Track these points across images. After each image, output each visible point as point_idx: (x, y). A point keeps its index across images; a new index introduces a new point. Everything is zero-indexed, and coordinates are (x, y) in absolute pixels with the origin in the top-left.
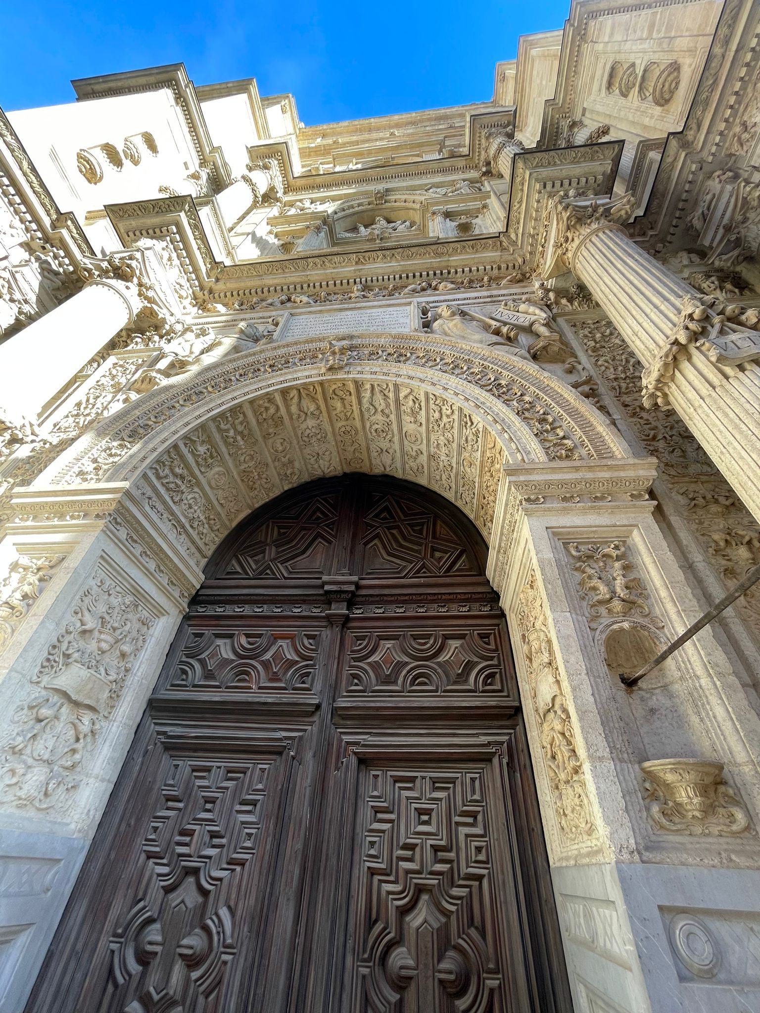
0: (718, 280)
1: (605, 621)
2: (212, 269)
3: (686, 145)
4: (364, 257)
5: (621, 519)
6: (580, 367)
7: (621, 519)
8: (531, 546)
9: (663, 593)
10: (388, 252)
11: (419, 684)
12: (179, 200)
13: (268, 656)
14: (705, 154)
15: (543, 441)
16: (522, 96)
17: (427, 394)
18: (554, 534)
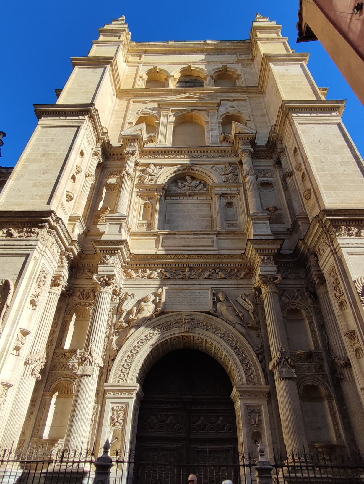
0: (310, 293)
2: (129, 255)
3: (305, 243)
4: (190, 256)
5: (259, 402)
7: (259, 402)
8: (240, 406)
9: (265, 423)
10: (199, 256)
11: (212, 431)
12: (122, 241)
13: (168, 422)
14: (310, 247)
15: (246, 374)
16: (264, 79)
17: (215, 345)
18: (246, 405)
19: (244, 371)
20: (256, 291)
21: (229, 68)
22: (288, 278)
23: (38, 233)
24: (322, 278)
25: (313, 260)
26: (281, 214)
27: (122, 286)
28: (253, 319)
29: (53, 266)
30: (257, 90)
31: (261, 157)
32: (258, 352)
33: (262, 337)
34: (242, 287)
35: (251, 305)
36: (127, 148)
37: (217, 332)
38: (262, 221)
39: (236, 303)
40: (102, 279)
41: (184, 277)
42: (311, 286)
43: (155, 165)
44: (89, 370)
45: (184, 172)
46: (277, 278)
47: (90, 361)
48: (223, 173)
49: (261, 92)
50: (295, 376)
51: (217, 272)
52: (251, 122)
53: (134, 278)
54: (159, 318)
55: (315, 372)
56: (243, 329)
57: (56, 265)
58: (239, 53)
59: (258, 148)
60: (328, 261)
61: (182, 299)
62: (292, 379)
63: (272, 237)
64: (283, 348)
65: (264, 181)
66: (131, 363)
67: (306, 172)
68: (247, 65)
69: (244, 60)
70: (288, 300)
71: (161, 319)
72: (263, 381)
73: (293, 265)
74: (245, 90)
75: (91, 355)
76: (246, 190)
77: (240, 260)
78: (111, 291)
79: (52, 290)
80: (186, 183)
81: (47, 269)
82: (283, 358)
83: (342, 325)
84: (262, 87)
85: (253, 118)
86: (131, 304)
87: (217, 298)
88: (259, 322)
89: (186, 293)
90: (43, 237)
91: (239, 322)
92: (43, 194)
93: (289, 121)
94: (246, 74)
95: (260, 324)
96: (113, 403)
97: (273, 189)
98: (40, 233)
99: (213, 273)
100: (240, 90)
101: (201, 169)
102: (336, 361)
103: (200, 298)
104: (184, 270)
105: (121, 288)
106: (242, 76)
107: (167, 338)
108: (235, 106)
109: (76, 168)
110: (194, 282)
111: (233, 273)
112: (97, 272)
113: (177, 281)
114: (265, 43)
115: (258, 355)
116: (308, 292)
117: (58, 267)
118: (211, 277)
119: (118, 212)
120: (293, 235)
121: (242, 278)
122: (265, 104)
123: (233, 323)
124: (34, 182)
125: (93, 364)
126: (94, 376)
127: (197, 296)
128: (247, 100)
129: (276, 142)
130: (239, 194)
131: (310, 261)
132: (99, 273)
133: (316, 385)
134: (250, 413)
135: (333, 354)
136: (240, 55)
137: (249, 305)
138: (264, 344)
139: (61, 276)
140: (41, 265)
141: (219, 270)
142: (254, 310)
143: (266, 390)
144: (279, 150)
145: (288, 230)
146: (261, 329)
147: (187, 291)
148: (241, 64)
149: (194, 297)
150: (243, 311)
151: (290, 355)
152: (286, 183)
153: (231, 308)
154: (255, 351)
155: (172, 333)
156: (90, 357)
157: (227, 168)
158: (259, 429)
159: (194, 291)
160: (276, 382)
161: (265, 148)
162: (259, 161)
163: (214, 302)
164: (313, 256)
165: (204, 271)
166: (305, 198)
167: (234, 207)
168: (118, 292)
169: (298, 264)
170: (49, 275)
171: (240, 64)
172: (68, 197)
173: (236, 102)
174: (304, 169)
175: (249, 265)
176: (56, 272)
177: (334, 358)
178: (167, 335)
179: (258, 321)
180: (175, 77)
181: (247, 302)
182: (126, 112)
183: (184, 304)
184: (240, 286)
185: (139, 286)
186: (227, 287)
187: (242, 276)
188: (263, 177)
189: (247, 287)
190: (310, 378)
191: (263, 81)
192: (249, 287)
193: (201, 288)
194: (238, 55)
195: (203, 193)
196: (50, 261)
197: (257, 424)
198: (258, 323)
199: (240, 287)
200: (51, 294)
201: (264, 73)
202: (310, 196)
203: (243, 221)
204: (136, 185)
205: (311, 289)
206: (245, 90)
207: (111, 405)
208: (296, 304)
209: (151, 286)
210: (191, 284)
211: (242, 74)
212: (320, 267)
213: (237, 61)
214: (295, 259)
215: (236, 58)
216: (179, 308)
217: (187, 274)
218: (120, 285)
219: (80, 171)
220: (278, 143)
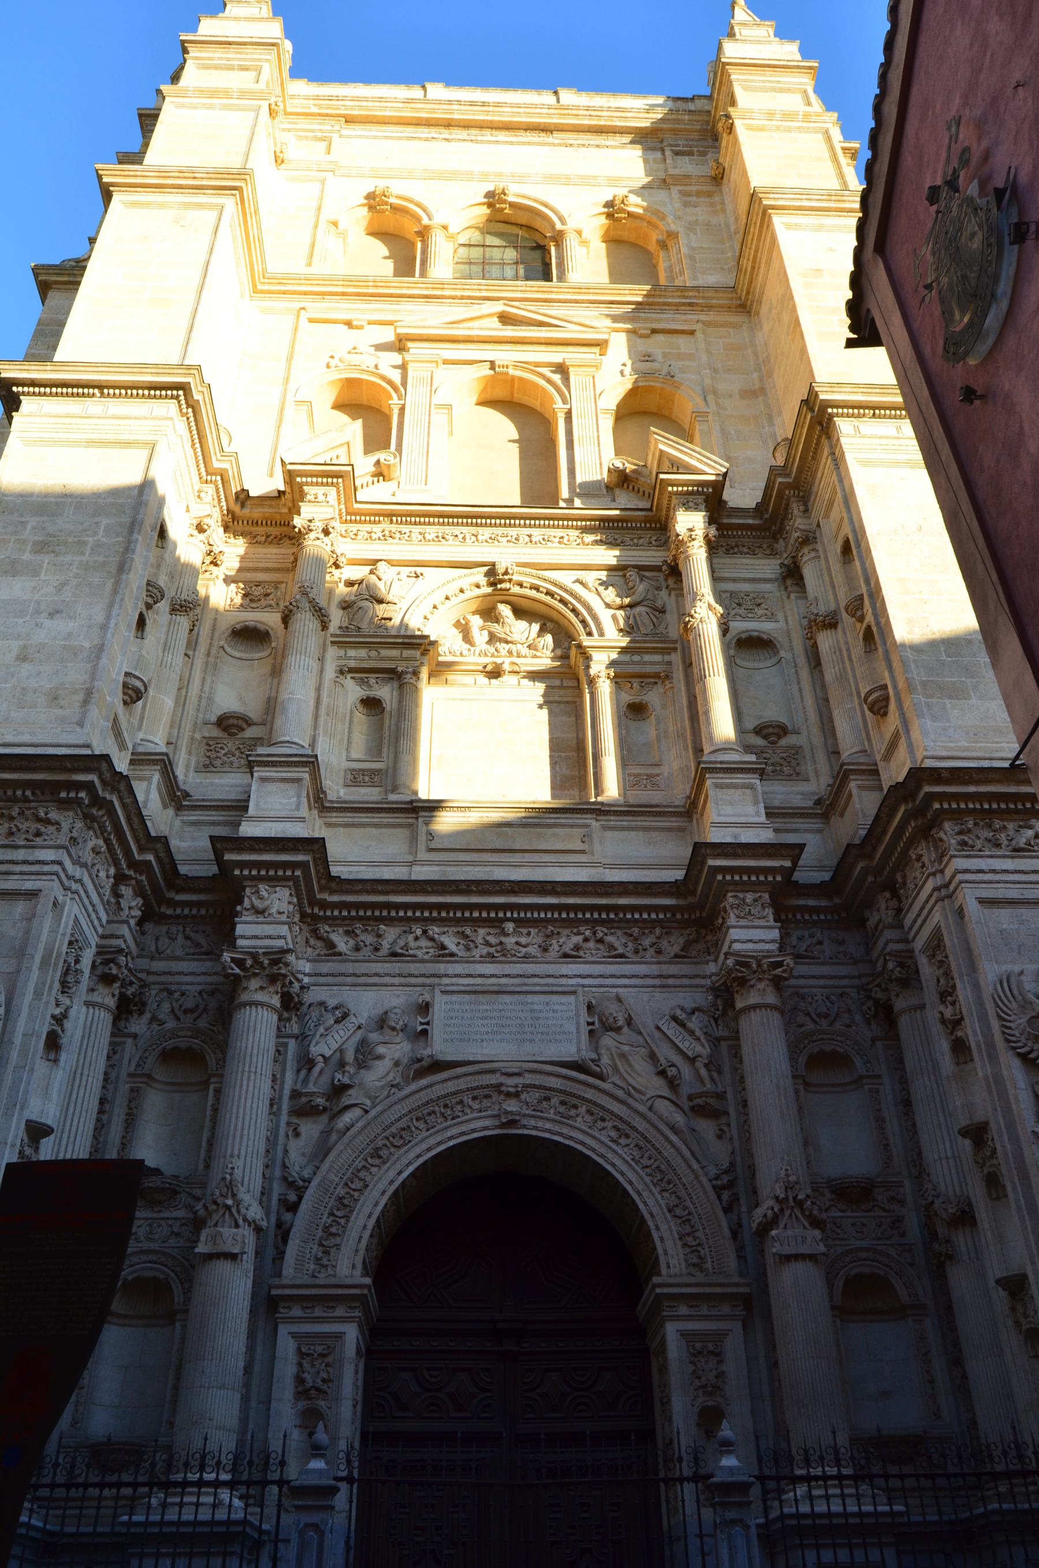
1: (700, 1400)
6: (728, 1136)
16: (753, 268)
19: (681, 1239)
20: (717, 997)
22: (813, 958)
23: (58, 823)
24: (910, 962)
25: (887, 908)
26: (797, 750)
27: (306, 980)
28: (708, 1085)
29: (96, 922)
30: (731, 299)
31: (741, 549)
32: (719, 1182)
33: (731, 1139)
34: (675, 986)
35: (702, 1038)
36: (302, 510)
37: (600, 1124)
38: (739, 779)
39: (657, 1035)
40: (249, 962)
41: (497, 952)
42: (879, 985)
46: (779, 964)
47: (231, 1213)
50: (822, 1248)
51: (600, 935)
52: (710, 418)
53: (340, 954)
54: (424, 1082)
55: (880, 1239)
56: (675, 1115)
57: (104, 918)
58: (671, 145)
59: (729, 516)
60: (927, 917)
61: (493, 1022)
62: (811, 1257)
63: (765, 836)
64: (790, 1172)
65: (747, 631)
66: (347, 1217)
67: (875, 629)
68: (699, 194)
69: (689, 177)
70: (811, 1026)
71: (431, 1086)
72: (732, 1262)
73: (829, 917)
74: (690, 297)
75: (234, 1196)
76: (691, 664)
78: (276, 1001)
79: (96, 998)
80: (496, 628)
81: (82, 932)
82: (791, 1199)
83: (958, 1103)
84: (748, 293)
85: (717, 404)
86: (337, 1036)
87: (601, 1021)
88: (725, 1092)
89: (506, 1003)
90: (75, 834)
91: (663, 1094)
92: (57, 688)
93: (831, 447)
94: (695, 234)
95: (726, 1100)
96: (295, 1336)
97: (774, 660)
98: (65, 826)
99: (586, 940)
100: (673, 297)
102: (936, 1205)
103: (548, 1018)
104: (498, 931)
105: (302, 988)
106: (682, 240)
107: (451, 1143)
108: (659, 355)
109: (148, 591)
110: (531, 968)
111: (647, 942)
112: (229, 938)
113: (478, 966)
114: (761, 129)
115: (718, 1190)
116: (870, 1003)
117: (108, 922)
118: (581, 953)
119: (288, 738)
120: (833, 820)
121: (676, 956)
122: (756, 354)
123: (648, 1096)
124: (22, 643)
125: (241, 1222)
126: (245, 1256)
127: (540, 1015)
128: (698, 334)
129: (787, 505)
130: (668, 677)
131: (878, 910)
132: (240, 942)
133: (882, 1273)
134: (694, 1355)
135: (930, 1186)
136: (677, 153)
138: (738, 1159)
139: (120, 951)
140: (71, 923)
141: (605, 930)
142: (711, 1056)
143: (742, 1290)
144: (798, 534)
145: (818, 802)
146: (728, 1114)
147: (507, 998)
148: (680, 192)
149: (529, 1014)
150: (677, 1059)
151: (809, 1191)
152: (815, 646)
153: (643, 1050)
154: (710, 1181)
155: (463, 1128)
156: (230, 1202)
157: (631, 584)
158: (720, 1399)
159: (530, 998)
160: (768, 1267)
161: (754, 518)
162: (733, 561)
163: (591, 1032)
164: (888, 895)
165: (558, 933)
166: (871, 709)
167: (653, 719)
168: (296, 1000)
169: (844, 915)
170: (88, 950)
171: (675, 190)
172: (130, 692)
173: (660, 337)
174: (869, 618)
175: (698, 914)
176: (103, 937)
177: (930, 1199)
178: (449, 1134)
179: (720, 1089)
180: (452, 229)
181: (692, 1033)
182: (290, 359)
183: (499, 1037)
184: (671, 981)
185: (360, 982)
186: (630, 986)
187: (676, 949)
188: (744, 618)
189: (691, 986)
190: (864, 1255)
191: (752, 273)
192: (697, 986)
193: (550, 989)
194: (668, 153)
196: (90, 909)
197: (713, 1386)
198: (721, 1096)
199: (669, 986)
200: (91, 1010)
201: (757, 251)
202: (887, 706)
203: (681, 769)
204: (332, 635)
205: (880, 995)
206: (690, 297)
207: (291, 1341)
208: (834, 1037)
209: (397, 980)
210: (521, 976)
211: (681, 229)
212: (906, 929)
213: (664, 181)
214: (837, 901)
215: (662, 166)
216: (485, 1051)
217: (510, 941)
218: (300, 976)
219: (158, 594)
220: (796, 509)
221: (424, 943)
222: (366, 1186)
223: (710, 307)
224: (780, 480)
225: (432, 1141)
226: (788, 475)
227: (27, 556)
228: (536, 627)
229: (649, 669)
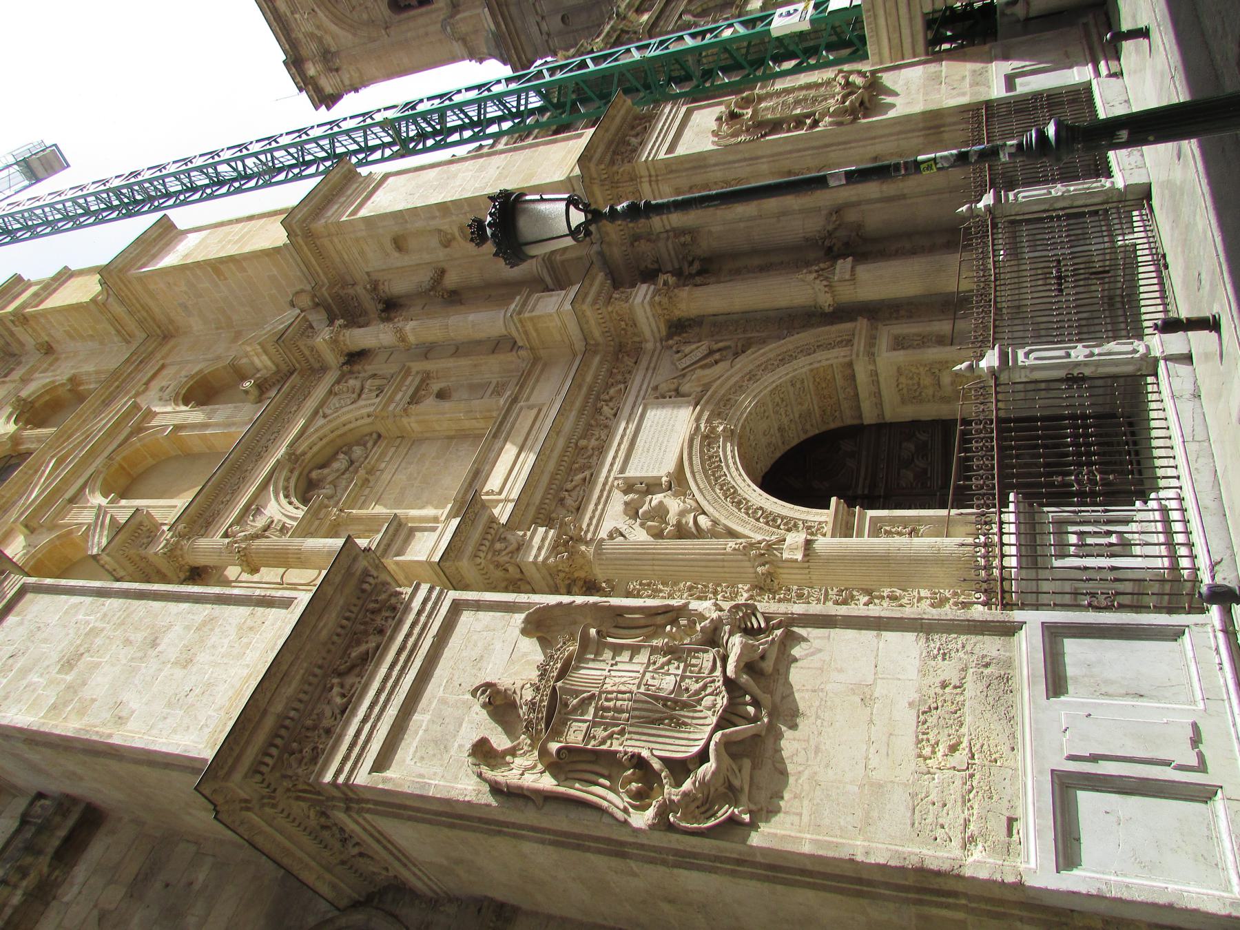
21: (29, 396)
43: (240, 520)
44: (797, 539)
45: (296, 473)
48: (355, 396)
49: (165, 337)
62: (853, 268)
66: (783, 518)
77: (597, 359)
80: (330, 479)
84: (159, 327)
101: (314, 437)
108: (164, 383)
128: (168, 361)
137: (700, 349)
184: (652, 365)
195: (379, 447)
209: (600, 507)
217: (593, 443)
221: (574, 494)
222: (761, 508)
223: (152, 353)
224: (324, 289)
225: (735, 474)
226: (323, 285)
227: (69, 678)
228: (341, 456)
229: (416, 383)
